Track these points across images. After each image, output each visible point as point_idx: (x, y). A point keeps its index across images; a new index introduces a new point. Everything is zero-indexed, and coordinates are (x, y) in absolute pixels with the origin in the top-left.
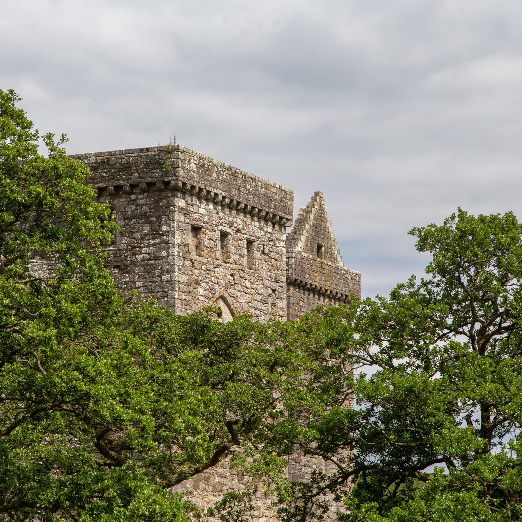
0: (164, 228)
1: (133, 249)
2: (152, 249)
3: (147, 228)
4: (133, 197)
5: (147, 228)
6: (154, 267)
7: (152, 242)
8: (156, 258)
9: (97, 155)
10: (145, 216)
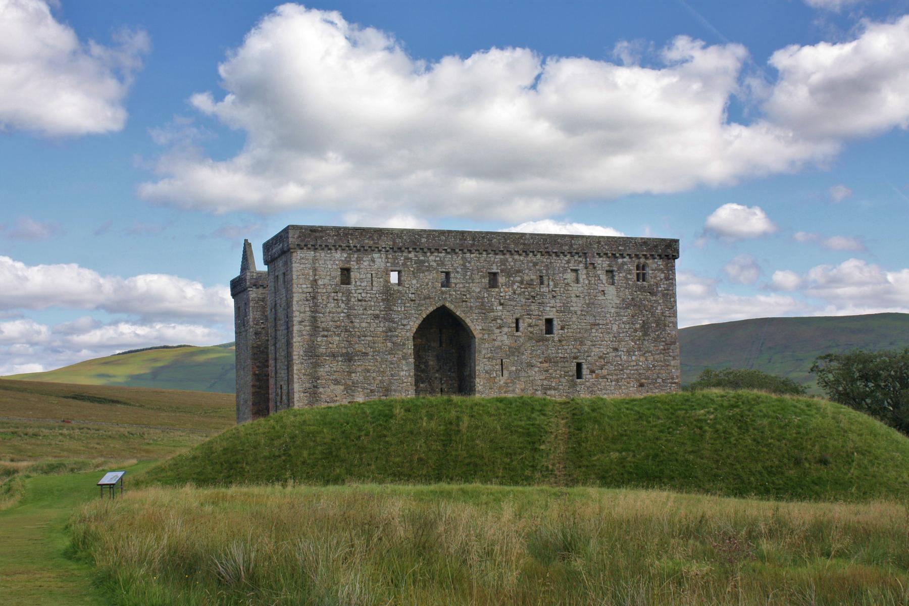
0: (671, 277)
1: (657, 285)
2: (665, 286)
3: (663, 276)
4: (656, 260)
5: (663, 276)
6: (667, 294)
7: (665, 282)
8: (668, 290)
9: (642, 239)
10: (662, 271)
